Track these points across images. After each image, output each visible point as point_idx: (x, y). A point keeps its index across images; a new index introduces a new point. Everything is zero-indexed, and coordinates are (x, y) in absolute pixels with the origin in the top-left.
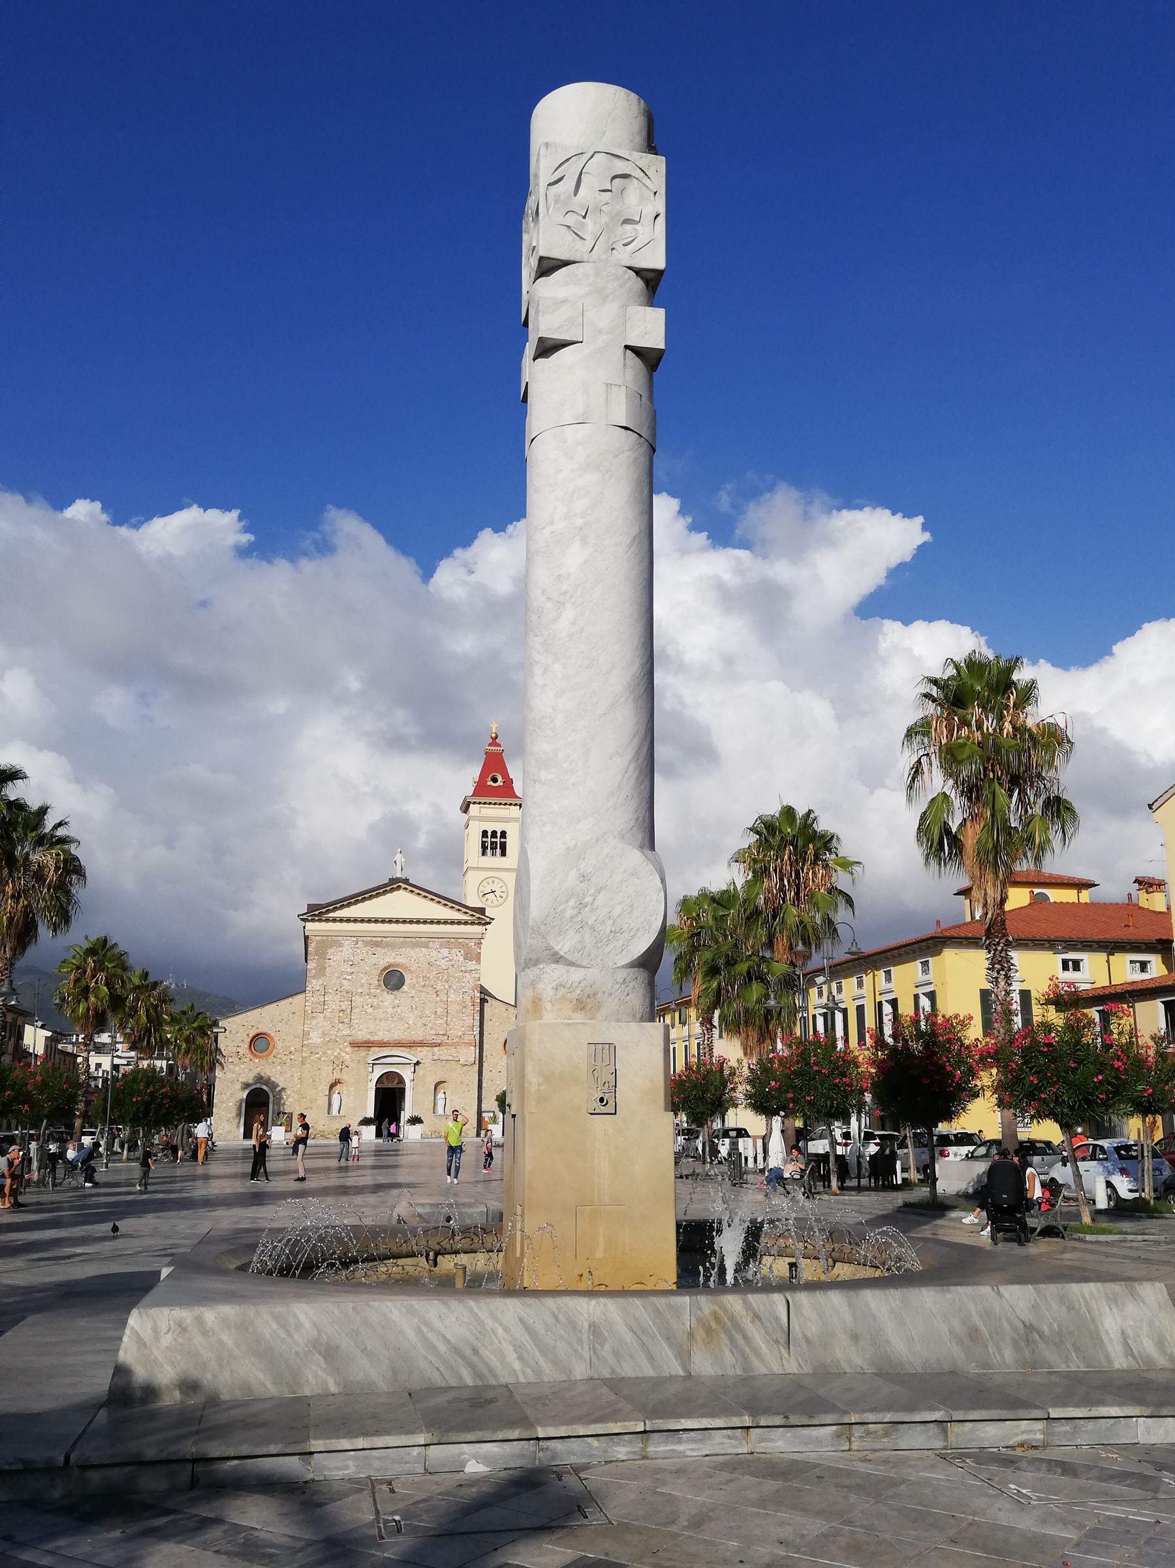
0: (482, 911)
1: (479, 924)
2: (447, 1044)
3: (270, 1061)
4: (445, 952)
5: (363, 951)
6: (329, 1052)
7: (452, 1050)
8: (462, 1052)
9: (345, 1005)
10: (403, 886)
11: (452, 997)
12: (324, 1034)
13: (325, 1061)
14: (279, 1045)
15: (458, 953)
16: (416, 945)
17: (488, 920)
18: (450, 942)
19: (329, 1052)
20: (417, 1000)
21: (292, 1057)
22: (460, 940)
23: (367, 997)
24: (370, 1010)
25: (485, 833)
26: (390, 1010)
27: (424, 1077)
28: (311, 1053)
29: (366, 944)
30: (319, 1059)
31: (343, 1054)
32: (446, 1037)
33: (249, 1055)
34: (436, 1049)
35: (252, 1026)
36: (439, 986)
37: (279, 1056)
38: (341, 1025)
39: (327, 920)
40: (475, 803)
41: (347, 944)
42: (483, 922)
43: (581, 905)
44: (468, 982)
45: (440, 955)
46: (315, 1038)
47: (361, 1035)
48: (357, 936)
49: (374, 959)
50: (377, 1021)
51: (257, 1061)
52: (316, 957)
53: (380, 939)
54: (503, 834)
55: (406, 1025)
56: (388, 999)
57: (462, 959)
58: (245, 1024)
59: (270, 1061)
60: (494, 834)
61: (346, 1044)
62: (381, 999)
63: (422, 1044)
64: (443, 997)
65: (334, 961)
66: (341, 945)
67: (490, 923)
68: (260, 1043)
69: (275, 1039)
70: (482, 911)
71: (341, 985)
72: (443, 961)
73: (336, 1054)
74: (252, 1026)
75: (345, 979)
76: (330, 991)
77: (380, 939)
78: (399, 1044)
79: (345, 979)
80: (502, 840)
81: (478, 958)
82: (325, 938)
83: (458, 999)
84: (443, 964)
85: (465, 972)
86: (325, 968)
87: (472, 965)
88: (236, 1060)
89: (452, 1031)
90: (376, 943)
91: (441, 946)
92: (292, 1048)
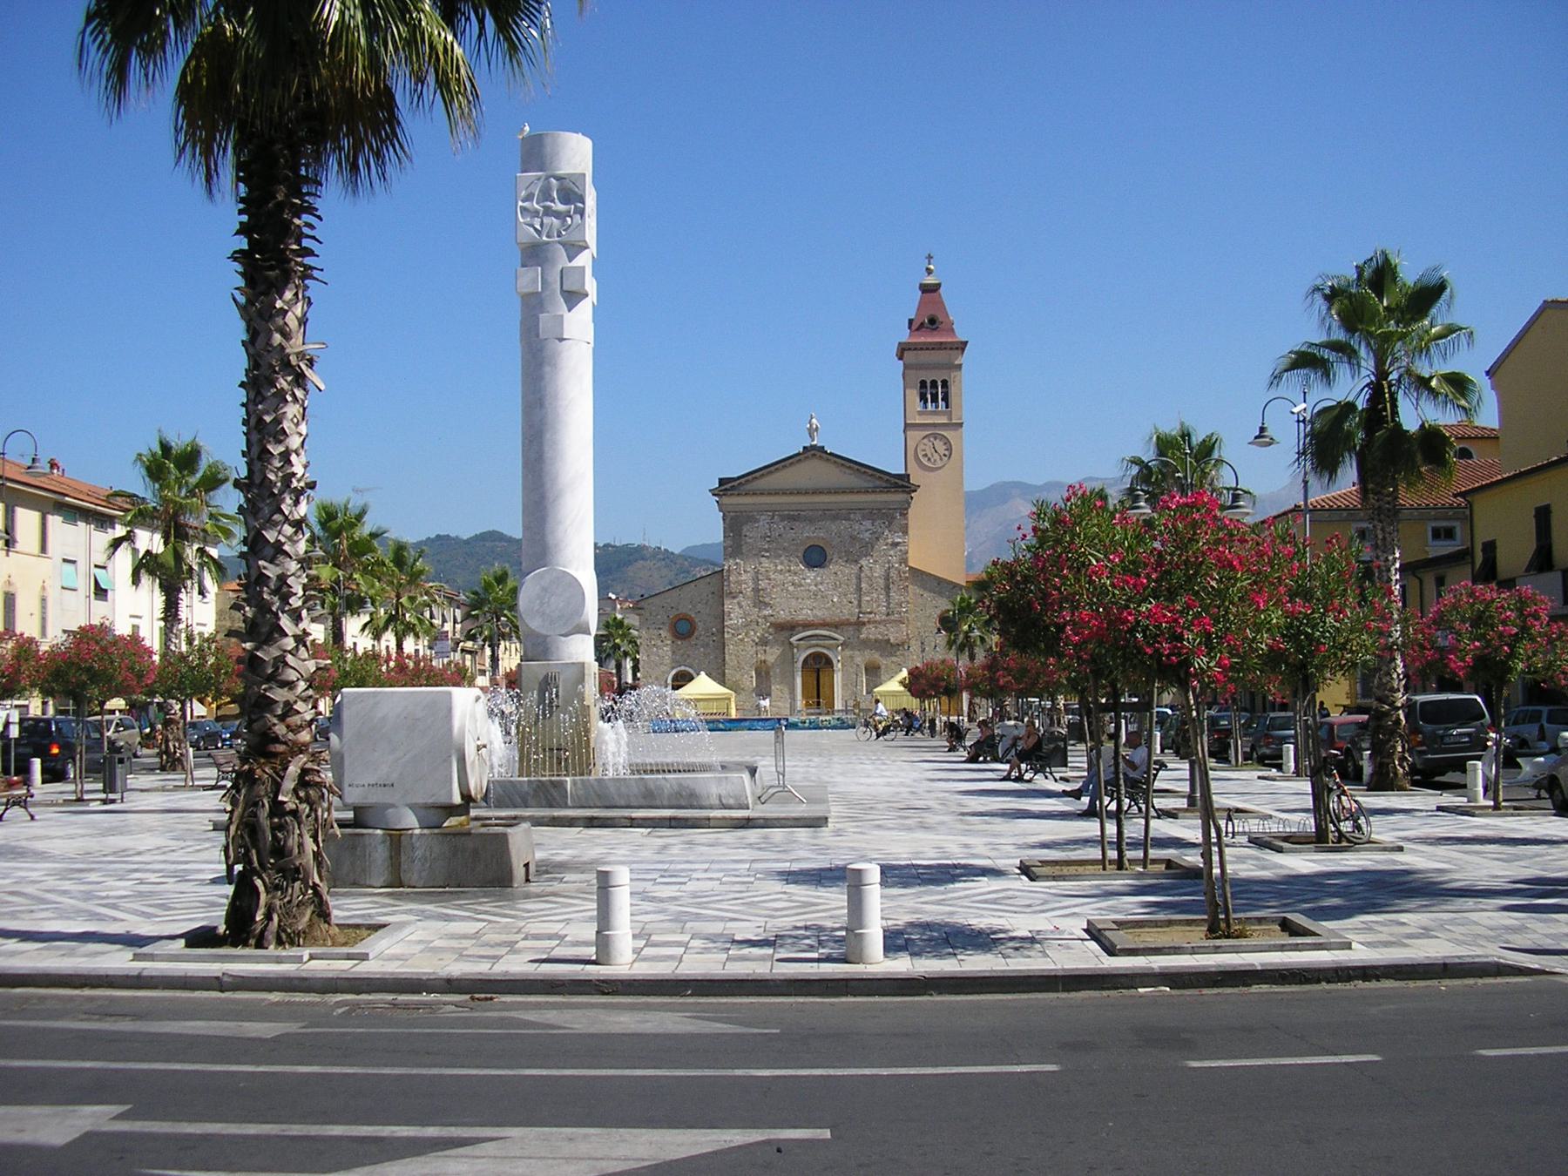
4: (868, 524)
5: (780, 527)
7: (882, 628)
10: (818, 454)
14: (700, 626)
16: (835, 518)
17: (913, 488)
24: (791, 588)
26: (813, 588)
41: (763, 520)
43: (542, 604)
45: (862, 528)
47: (783, 616)
48: (773, 512)
53: (796, 513)
56: (811, 575)
65: (750, 538)
66: (757, 521)
68: (683, 627)
69: (697, 620)
75: (763, 556)
77: (796, 513)
78: (824, 625)
88: (659, 643)
90: (793, 518)
91: (864, 518)
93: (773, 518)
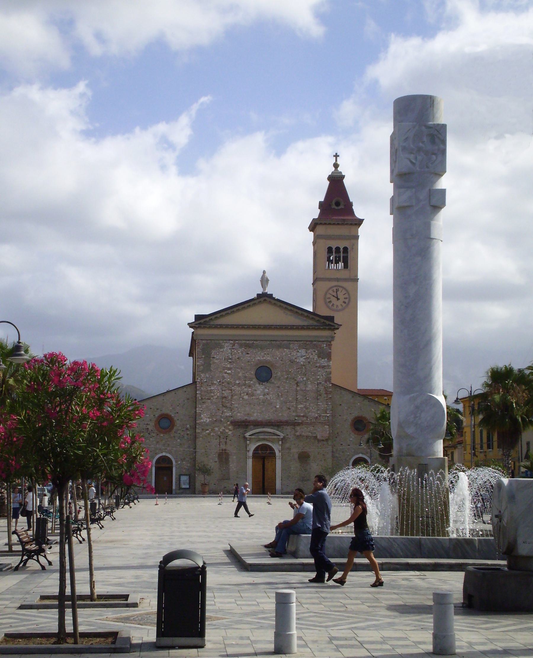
0: (331, 319)
1: (329, 329)
2: (307, 424)
3: (172, 435)
5: (239, 351)
6: (217, 429)
7: (311, 428)
8: (319, 430)
9: (226, 393)
11: (309, 387)
12: (212, 416)
13: (213, 435)
15: (313, 353)
16: (279, 347)
18: (307, 344)
19: (217, 429)
20: (282, 389)
21: (188, 432)
22: (314, 343)
23: (243, 387)
24: (246, 397)
25: (330, 250)
27: (289, 449)
28: (203, 429)
29: (241, 346)
30: (209, 434)
31: (227, 431)
32: (305, 418)
33: (156, 431)
34: (298, 428)
35: (157, 409)
36: (299, 378)
37: (179, 432)
38: (224, 408)
39: (210, 327)
40: (321, 224)
41: (227, 347)
42: (333, 328)
44: (321, 375)
45: (299, 354)
46: (205, 418)
47: (240, 416)
48: (234, 340)
49: (247, 357)
50: (252, 406)
51: (162, 435)
52: (203, 356)
53: (251, 342)
54: (346, 249)
55: (274, 409)
56: (260, 389)
57: (316, 357)
58: (152, 407)
59: (172, 435)
60: (338, 249)
61: (229, 423)
62: (254, 388)
63: (287, 423)
64: (302, 386)
65: (217, 359)
66: (222, 347)
67: (338, 329)
68: (165, 423)
69: (175, 419)
70: (331, 319)
71: (224, 378)
72: (301, 359)
73: (221, 430)
74: (157, 409)
75: (226, 373)
76: (215, 382)
77: (251, 342)
79: (226, 373)
80: (345, 255)
81: (328, 356)
82: (209, 341)
83: (314, 388)
84: (302, 360)
85: (319, 367)
86: (211, 364)
87: (323, 362)
89: (310, 414)
92: (188, 426)
93: (234, 345)
